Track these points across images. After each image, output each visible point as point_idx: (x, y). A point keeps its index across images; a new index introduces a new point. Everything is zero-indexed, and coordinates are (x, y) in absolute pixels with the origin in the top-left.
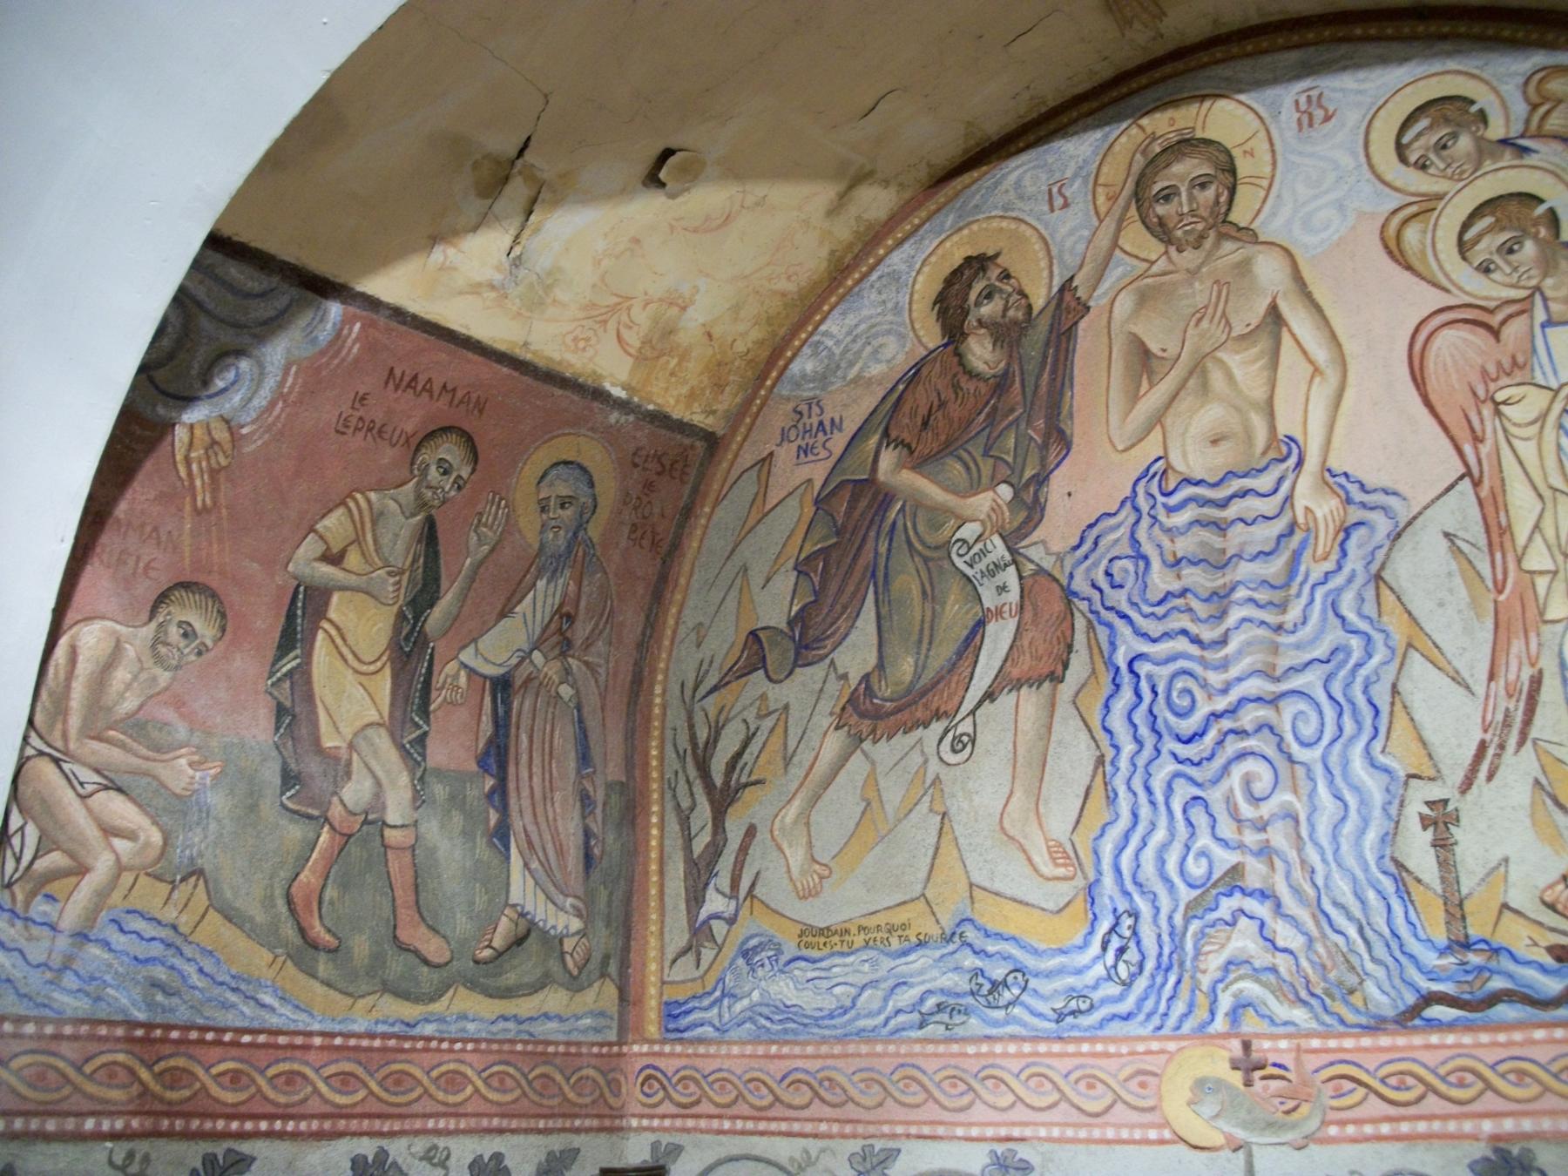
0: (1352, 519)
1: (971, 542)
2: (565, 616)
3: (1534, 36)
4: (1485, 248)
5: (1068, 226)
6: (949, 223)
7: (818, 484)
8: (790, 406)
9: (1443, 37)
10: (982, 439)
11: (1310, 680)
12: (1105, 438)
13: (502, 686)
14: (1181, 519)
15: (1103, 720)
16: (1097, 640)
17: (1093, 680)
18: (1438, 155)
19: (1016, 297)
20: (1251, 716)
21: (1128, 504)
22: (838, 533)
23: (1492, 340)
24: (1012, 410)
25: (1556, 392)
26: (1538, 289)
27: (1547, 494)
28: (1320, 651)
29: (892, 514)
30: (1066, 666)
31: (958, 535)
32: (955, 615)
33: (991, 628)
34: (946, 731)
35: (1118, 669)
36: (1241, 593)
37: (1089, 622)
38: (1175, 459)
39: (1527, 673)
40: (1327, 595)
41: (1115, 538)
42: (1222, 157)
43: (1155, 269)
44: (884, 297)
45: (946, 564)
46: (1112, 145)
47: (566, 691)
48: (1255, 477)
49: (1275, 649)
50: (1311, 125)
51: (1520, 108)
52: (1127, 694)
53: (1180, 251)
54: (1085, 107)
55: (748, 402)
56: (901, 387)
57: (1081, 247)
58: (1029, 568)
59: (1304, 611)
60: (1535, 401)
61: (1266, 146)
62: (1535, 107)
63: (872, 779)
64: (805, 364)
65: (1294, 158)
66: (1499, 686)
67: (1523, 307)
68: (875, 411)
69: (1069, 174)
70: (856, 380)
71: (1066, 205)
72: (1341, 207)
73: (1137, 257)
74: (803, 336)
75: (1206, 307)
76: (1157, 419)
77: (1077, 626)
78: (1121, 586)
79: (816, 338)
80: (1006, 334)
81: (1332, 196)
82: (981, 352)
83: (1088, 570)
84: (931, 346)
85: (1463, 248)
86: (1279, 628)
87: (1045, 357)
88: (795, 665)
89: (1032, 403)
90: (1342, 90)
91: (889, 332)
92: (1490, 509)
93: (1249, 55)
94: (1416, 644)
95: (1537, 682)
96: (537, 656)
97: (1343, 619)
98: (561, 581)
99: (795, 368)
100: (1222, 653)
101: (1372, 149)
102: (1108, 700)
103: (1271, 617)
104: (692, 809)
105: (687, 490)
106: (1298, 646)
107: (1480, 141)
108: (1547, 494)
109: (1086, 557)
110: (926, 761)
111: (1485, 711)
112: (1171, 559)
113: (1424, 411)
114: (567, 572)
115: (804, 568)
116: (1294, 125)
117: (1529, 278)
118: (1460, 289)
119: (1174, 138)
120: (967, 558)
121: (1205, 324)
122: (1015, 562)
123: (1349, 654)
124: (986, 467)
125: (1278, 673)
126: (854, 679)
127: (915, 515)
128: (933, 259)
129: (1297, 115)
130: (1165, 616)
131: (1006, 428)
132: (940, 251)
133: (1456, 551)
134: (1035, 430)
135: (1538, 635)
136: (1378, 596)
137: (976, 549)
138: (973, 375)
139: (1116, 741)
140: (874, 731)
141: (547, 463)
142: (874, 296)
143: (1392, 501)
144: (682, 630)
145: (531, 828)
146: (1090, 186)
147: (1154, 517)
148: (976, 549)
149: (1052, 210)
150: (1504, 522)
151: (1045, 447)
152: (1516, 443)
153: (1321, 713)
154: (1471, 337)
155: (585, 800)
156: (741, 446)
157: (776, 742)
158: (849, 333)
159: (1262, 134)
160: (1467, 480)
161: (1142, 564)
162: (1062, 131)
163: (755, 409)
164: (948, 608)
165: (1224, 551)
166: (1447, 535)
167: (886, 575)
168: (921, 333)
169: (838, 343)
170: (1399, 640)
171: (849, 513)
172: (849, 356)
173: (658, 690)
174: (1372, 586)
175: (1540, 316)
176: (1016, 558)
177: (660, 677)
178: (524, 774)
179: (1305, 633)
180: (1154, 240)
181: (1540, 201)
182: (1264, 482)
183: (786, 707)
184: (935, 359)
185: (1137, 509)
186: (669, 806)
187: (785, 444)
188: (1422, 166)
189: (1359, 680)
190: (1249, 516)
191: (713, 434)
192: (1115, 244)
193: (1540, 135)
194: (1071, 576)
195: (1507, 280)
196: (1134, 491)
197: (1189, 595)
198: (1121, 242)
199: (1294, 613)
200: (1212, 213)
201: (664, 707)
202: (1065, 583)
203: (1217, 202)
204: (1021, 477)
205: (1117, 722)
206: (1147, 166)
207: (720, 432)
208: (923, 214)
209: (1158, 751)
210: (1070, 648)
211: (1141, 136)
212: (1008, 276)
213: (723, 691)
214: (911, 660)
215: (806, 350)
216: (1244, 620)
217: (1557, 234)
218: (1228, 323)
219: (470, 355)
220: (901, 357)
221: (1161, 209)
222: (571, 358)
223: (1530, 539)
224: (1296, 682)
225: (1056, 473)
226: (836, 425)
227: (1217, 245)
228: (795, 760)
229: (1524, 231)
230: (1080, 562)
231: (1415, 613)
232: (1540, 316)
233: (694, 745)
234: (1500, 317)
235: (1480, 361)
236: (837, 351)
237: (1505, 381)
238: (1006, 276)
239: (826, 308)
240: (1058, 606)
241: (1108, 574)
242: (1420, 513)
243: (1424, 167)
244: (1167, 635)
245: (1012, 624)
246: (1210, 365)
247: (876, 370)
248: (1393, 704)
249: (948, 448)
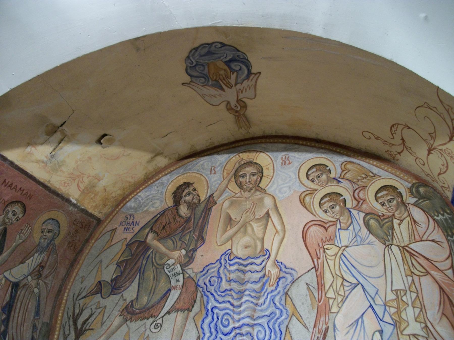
0: (281, 275)
1: (171, 265)
2: (41, 266)
3: (345, 152)
4: (326, 206)
5: (215, 179)
6: (181, 172)
7: (128, 240)
8: (125, 215)
9: (322, 148)
11: (263, 321)
12: (215, 241)
13: (16, 286)
14: (233, 268)
15: (201, 325)
16: (203, 300)
17: (200, 312)
18: (317, 179)
19: (196, 196)
20: (245, 330)
21: (219, 262)
22: (132, 256)
23: (326, 231)
24: (190, 228)
25: (340, 248)
26: (339, 219)
27: (335, 276)
28: (267, 313)
29: (149, 253)
30: (193, 307)
31: (167, 262)
32: (162, 286)
33: (172, 292)
34: (154, 322)
35: (208, 310)
36: (247, 293)
37: (202, 295)
39: (324, 327)
40: (271, 297)
41: (213, 270)
42: (260, 169)
43: (237, 196)
44: (158, 189)
45: (162, 270)
46: (230, 159)
47: (36, 290)
48: (256, 259)
49: (255, 310)
50: (285, 164)
51: (339, 170)
52: (210, 318)
53: (244, 192)
54: (225, 148)
55: (112, 212)
56: (159, 216)
57: (217, 186)
58: (187, 276)
59: (264, 300)
60: (335, 250)
61: (272, 168)
62: (343, 171)
63: (128, 333)
64: (131, 204)
65: (279, 172)
66: (316, 330)
67: (334, 224)
68: (149, 221)
69: (217, 165)
70: (146, 212)
71: (215, 173)
72: (290, 188)
73: (232, 191)
74: (133, 195)
75: (249, 209)
76: (231, 238)
77: (198, 295)
78: (213, 285)
79: (136, 197)
80: (192, 206)
81: (288, 185)
82: (184, 210)
83: (204, 279)
84: (170, 205)
85: (320, 205)
86: (257, 304)
87: (202, 215)
88: (111, 294)
89: (196, 228)
90: (295, 157)
91: (158, 199)
92: (319, 278)
93: (271, 143)
94: (295, 314)
95: (327, 330)
96: (29, 278)
97: (275, 304)
98: (43, 255)
99: (128, 204)
100: (239, 310)
101: (300, 174)
102: (204, 319)
103: (255, 301)
104: (69, 335)
105: (88, 235)
106: (261, 311)
107: (328, 177)
108: (335, 276)
109: (204, 275)
110: (146, 330)
111: (312, 337)
112: (228, 279)
113: (305, 248)
114: (45, 253)
115: (119, 265)
116: (281, 164)
117: (337, 216)
118: (319, 216)
119: (248, 161)
120: (169, 270)
121: (248, 213)
122: (183, 273)
123: (275, 315)
124: (179, 244)
125: (255, 318)
126: (128, 301)
127: (156, 254)
128: (175, 181)
129: (281, 161)
130: (224, 296)
131: (187, 233)
132: (177, 179)
133: (309, 289)
134: (195, 235)
135: (329, 316)
136: (286, 299)
137: (172, 267)
138: (180, 216)
139: (204, 332)
140: (131, 318)
141: (47, 218)
142: (156, 188)
143: (293, 272)
144: (77, 278)
145: (14, 334)
146: (223, 169)
147: (225, 266)
148: (172, 267)
149: (211, 174)
150: (323, 283)
151: (197, 241)
152: (328, 260)
153: (265, 331)
154: (320, 229)
155: (34, 327)
157: (100, 317)
158: (146, 197)
159: (272, 164)
160: (314, 269)
161: (220, 280)
162: (217, 153)
163: (114, 214)
164: (161, 284)
165: (244, 279)
166: (307, 284)
167: (144, 271)
168: (167, 201)
169: (142, 199)
170: (290, 313)
171: (136, 251)
172: (145, 204)
173: (66, 295)
174: (284, 296)
175: (338, 226)
177: (67, 291)
178: (16, 315)
179: (264, 307)
180: (238, 188)
181: (342, 196)
182: (258, 261)
183: (105, 307)
184: (170, 210)
185: (221, 263)
186: (62, 332)
187: (121, 226)
189: (278, 323)
190: (253, 270)
191: (100, 219)
192: (227, 187)
193: (343, 178)
194: (199, 280)
195: (331, 216)
196: (221, 258)
197: (232, 291)
198: (228, 186)
199: (261, 301)
200: (255, 183)
201: (67, 301)
202: (196, 282)
203: (257, 180)
204: (189, 248)
205: (205, 326)
206: (239, 167)
207: (102, 219)
208: (174, 168)
209: (216, 337)
210: (195, 301)
211: (239, 158)
212: (195, 190)
213: (87, 298)
214: (146, 298)
215: (133, 200)
216: (247, 301)
217: (345, 206)
218: (254, 214)
219: (31, 181)
220: (160, 207)
221: (241, 179)
222: (62, 188)
223: (329, 288)
224: (259, 321)
225: (199, 249)
227: (255, 192)
228: (105, 324)
229: (337, 203)
230: (202, 276)
231: (295, 305)
232: (338, 226)
233: (74, 315)
234: (328, 225)
235: (321, 236)
236: (142, 202)
237: (327, 243)
238: (195, 190)
239: (141, 189)
240: (193, 289)
241: (209, 281)
242: (300, 277)
243: (313, 181)
244: (224, 302)
245: (179, 292)
246: (248, 225)
247: (152, 209)
248: (286, 331)
249: (169, 236)
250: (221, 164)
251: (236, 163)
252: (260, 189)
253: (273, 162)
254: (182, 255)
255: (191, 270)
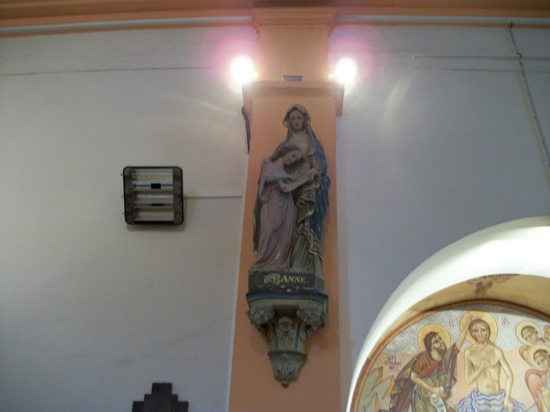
10: (436, 375)
14: (481, 402)
19: (442, 344)
22: (402, 390)
24: (443, 370)
38: (480, 389)
41: (468, 403)
45: (429, 402)
51: (543, 333)
54: (457, 305)
57: (457, 337)
58: (448, 407)
61: (496, 326)
64: (390, 346)
67: (545, 373)
69: (454, 319)
75: (485, 358)
79: (393, 341)
80: (442, 352)
107: (537, 337)
118: (534, 366)
119: (477, 318)
121: (485, 361)
128: (423, 330)
134: (448, 376)
138: (433, 359)
142: (408, 334)
144: (360, 407)
146: (459, 323)
152: (545, 399)
156: (374, 363)
159: (495, 323)
169: (399, 343)
176: (445, 404)
182: (498, 398)
188: (526, 339)
193: (547, 339)
196: (471, 394)
198: (466, 338)
215: (391, 343)
221: (475, 333)
226: (399, 364)
238: (440, 338)
247: (409, 353)
250: (456, 319)
251: (468, 320)
252: (490, 343)
253: (495, 321)
254: (441, 391)
255: (451, 403)
